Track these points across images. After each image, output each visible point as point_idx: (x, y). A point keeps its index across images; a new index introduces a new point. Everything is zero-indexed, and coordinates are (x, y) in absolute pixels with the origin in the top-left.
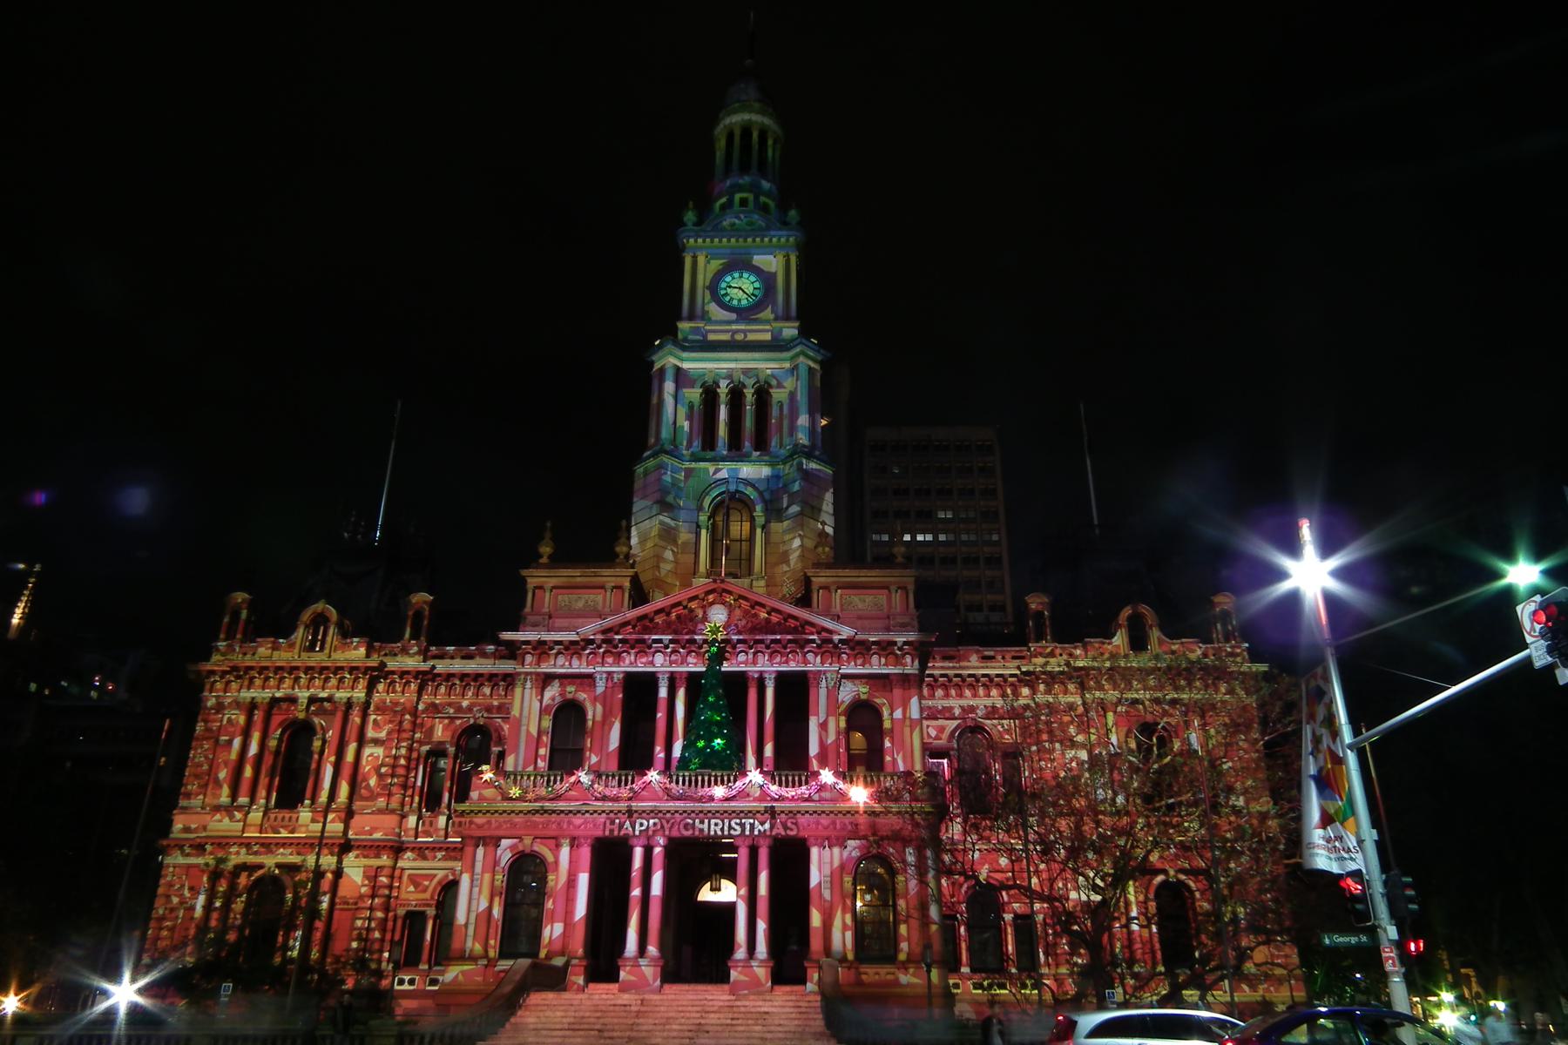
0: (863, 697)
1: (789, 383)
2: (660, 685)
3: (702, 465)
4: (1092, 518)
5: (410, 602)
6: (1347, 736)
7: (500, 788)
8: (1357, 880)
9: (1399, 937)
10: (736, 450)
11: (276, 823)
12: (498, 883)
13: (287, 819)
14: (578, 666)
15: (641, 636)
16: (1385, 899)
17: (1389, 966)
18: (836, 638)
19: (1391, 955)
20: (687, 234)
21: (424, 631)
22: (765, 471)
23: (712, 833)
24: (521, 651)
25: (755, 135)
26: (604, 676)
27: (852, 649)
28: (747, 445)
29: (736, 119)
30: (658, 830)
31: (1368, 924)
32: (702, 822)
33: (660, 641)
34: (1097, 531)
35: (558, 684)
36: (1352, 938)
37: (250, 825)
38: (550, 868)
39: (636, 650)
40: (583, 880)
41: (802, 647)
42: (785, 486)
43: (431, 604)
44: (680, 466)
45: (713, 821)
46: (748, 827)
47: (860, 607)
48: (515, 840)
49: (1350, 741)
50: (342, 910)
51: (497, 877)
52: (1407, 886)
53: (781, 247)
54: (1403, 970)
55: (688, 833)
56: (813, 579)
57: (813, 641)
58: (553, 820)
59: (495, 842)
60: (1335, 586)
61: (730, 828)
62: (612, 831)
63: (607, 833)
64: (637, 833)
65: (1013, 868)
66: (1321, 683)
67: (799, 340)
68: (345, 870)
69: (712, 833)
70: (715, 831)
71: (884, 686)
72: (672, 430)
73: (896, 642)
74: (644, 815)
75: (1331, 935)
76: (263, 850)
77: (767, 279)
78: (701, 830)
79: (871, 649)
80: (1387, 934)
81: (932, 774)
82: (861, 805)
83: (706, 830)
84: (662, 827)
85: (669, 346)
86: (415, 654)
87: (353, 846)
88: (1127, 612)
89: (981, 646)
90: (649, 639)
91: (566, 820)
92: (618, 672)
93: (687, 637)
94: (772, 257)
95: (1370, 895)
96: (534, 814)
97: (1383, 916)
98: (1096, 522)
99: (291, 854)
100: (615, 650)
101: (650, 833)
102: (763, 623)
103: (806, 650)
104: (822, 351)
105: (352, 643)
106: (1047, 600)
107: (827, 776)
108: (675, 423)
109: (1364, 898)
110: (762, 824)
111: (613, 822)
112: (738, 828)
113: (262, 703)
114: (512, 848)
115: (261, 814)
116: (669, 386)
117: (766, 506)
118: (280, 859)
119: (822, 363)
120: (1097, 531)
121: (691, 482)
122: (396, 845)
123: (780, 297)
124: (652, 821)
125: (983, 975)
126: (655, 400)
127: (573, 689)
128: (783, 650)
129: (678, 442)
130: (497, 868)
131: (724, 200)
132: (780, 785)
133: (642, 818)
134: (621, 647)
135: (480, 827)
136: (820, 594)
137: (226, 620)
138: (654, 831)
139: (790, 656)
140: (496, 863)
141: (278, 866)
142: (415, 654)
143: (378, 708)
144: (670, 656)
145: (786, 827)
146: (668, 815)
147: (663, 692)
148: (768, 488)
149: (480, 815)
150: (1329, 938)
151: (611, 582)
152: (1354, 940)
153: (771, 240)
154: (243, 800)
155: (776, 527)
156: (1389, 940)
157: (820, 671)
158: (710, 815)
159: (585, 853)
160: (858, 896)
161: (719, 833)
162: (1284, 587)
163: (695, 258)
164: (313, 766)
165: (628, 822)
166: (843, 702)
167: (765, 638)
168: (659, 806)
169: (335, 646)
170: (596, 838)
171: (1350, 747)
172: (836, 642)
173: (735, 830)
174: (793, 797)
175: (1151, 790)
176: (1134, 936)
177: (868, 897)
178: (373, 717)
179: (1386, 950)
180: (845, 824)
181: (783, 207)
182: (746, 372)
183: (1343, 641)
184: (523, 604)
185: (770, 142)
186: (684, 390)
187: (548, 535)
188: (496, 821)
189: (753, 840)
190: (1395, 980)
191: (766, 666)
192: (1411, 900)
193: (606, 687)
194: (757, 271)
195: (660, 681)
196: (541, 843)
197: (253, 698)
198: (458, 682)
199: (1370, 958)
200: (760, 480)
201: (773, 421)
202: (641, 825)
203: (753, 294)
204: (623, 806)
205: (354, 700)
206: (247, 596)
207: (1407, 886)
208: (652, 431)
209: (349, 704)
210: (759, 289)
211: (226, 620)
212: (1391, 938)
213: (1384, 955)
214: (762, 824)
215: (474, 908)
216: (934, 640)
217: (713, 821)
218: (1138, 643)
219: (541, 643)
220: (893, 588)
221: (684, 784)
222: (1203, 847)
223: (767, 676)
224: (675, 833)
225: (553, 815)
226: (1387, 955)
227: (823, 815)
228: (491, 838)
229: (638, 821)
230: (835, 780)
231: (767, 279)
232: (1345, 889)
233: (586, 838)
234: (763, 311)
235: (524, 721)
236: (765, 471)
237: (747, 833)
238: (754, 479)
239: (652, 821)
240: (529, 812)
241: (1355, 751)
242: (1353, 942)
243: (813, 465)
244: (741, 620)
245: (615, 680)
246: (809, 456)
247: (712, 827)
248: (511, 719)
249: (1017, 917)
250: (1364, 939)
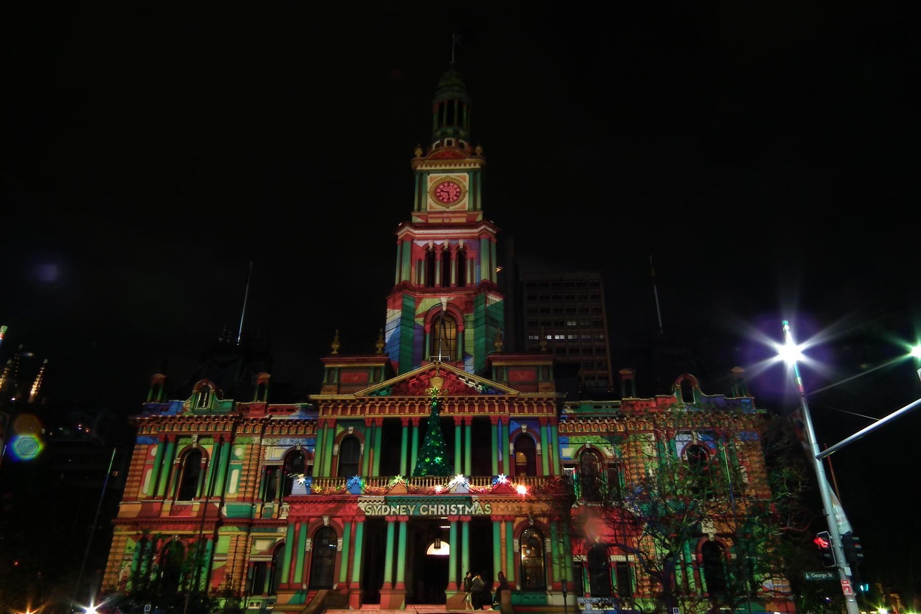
4: (659, 323)
6: (816, 451)
8: (824, 539)
9: (852, 574)
16: (843, 550)
17: (846, 592)
19: (848, 585)
25: (456, 105)
29: (444, 96)
31: (832, 566)
34: (662, 331)
36: (823, 575)
44: (414, 296)
49: (818, 454)
52: (856, 542)
54: (855, 594)
60: (805, 359)
66: (800, 419)
75: (809, 573)
80: (845, 573)
81: (566, 477)
82: (524, 496)
87: (224, 522)
88: (681, 379)
94: (467, 174)
95: (833, 548)
97: (842, 561)
98: (661, 326)
102: (464, 388)
104: (497, 228)
107: (502, 479)
109: (829, 550)
120: (662, 331)
122: (249, 521)
125: (599, 599)
131: (438, 142)
132: (475, 484)
135: (298, 511)
150: (808, 575)
152: (824, 576)
156: (846, 576)
160: (523, 551)
162: (775, 360)
171: (818, 457)
174: (482, 491)
175: (697, 485)
176: (689, 575)
177: (528, 552)
179: (844, 582)
180: (514, 508)
181: (473, 145)
183: (812, 393)
184: (323, 380)
185: (465, 108)
187: (337, 338)
189: (459, 518)
190: (850, 600)
192: (858, 551)
199: (835, 587)
207: (856, 542)
212: (847, 575)
213: (843, 585)
216: (565, 397)
218: (688, 398)
221: (418, 484)
222: (730, 520)
226: (845, 585)
227: (501, 503)
230: (507, 481)
232: (818, 545)
240: (326, 501)
241: (821, 460)
242: (824, 577)
244: (450, 386)
250: (830, 575)
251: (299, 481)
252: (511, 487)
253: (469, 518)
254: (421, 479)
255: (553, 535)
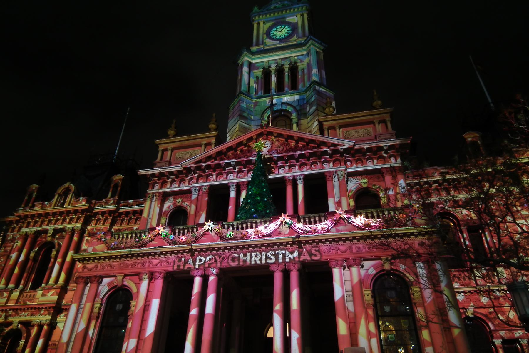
0: (365, 185)
1: (306, 60)
2: (231, 190)
3: (263, 99)
5: (113, 179)
7: (106, 243)
10: (281, 90)
11: (26, 299)
12: (96, 310)
13: (32, 296)
14: (185, 187)
15: (217, 162)
18: (341, 148)
20: (255, 15)
21: (117, 194)
22: (297, 97)
23: (253, 263)
24: (151, 182)
26: (197, 188)
27: (353, 156)
28: (286, 89)
30: (212, 263)
32: (245, 255)
33: (229, 165)
35: (172, 199)
37: (12, 300)
38: (134, 297)
39: (217, 172)
40: (155, 303)
41: (320, 158)
42: (308, 102)
43: (123, 180)
44: (251, 101)
45: (253, 254)
46: (281, 256)
47: (356, 136)
48: (112, 279)
50: (52, 349)
51: (96, 306)
53: (298, 12)
55: (234, 264)
56: (324, 123)
57: (326, 153)
58: (139, 261)
59: (99, 279)
61: (267, 257)
62: (179, 266)
63: (175, 268)
64: (197, 266)
65: (493, 304)
67: (309, 38)
68: (58, 324)
69: (253, 263)
70: (255, 261)
71: (379, 178)
72: (247, 87)
73: (383, 146)
74: (203, 253)
76: (14, 313)
77: (294, 27)
78: (245, 261)
79: (366, 156)
83: (248, 260)
84: (216, 261)
85: (245, 52)
86: (112, 204)
87: (63, 309)
89: (438, 166)
90: (223, 163)
91: (148, 261)
92: (206, 186)
93: (246, 159)
94: (295, 17)
96: (126, 258)
99: (28, 315)
100: (204, 174)
101: (207, 266)
103: (322, 160)
104: (322, 43)
105: (79, 200)
106: (478, 135)
108: (249, 84)
110: (292, 253)
111: (180, 260)
112: (273, 257)
113: (31, 234)
114: (109, 284)
115: (18, 293)
116: (245, 69)
117: (298, 113)
118: (22, 319)
119: (323, 50)
121: (257, 108)
123: (300, 30)
124: (208, 258)
126: (239, 78)
127: (180, 200)
128: (307, 162)
129: (251, 92)
130: (97, 299)
132: (305, 223)
133: (201, 256)
134: (208, 172)
135: (90, 270)
136: (329, 132)
137: (26, 198)
138: (209, 264)
139: (312, 166)
140: (96, 295)
141: (21, 322)
142: (112, 204)
143: (90, 235)
144: (237, 175)
145: (311, 254)
146: (220, 252)
147: (233, 194)
148: (298, 105)
149: (91, 261)
151: (204, 141)
153: (294, 10)
154: (11, 286)
155: (303, 121)
157: (333, 171)
158: (251, 249)
159: (159, 283)
161: (258, 262)
163: (258, 24)
164: (50, 265)
165: (191, 259)
166: (350, 191)
167: (295, 153)
168: (212, 245)
169: (72, 204)
170: (167, 272)
172: (342, 150)
173: (271, 259)
178: (86, 238)
180: (359, 248)
182: (284, 59)
184: (156, 159)
186: (254, 71)
187: (173, 126)
188: (101, 265)
189: (285, 266)
191: (298, 172)
193: (198, 195)
194: (289, 24)
195: (231, 188)
196: (130, 279)
197: (27, 232)
198: (132, 217)
200: (294, 101)
201: (300, 77)
202: (200, 260)
203: (287, 33)
204: (185, 247)
205: (76, 228)
206: (37, 186)
208: (238, 88)
209: (73, 230)
210: (290, 30)
211: (26, 198)
214: (292, 253)
215: (75, 330)
216: (409, 142)
217: (253, 254)
219: (162, 175)
220: (376, 121)
221: (233, 229)
223: (298, 178)
224: (225, 265)
225: (140, 258)
227: (341, 243)
228: (96, 277)
229: (198, 258)
231: (294, 27)
233: (160, 272)
234: (292, 37)
235: (149, 220)
236: (297, 97)
237: (280, 260)
238: (291, 101)
239: (208, 258)
243: (321, 89)
245: (204, 190)
246: (320, 84)
247: (253, 258)
248: (142, 219)
249: (505, 342)
251: (96, 236)
252: (352, 221)
253: (297, 266)
254: (237, 224)
255: (422, 281)
